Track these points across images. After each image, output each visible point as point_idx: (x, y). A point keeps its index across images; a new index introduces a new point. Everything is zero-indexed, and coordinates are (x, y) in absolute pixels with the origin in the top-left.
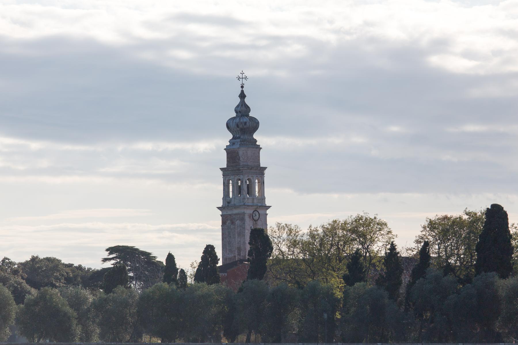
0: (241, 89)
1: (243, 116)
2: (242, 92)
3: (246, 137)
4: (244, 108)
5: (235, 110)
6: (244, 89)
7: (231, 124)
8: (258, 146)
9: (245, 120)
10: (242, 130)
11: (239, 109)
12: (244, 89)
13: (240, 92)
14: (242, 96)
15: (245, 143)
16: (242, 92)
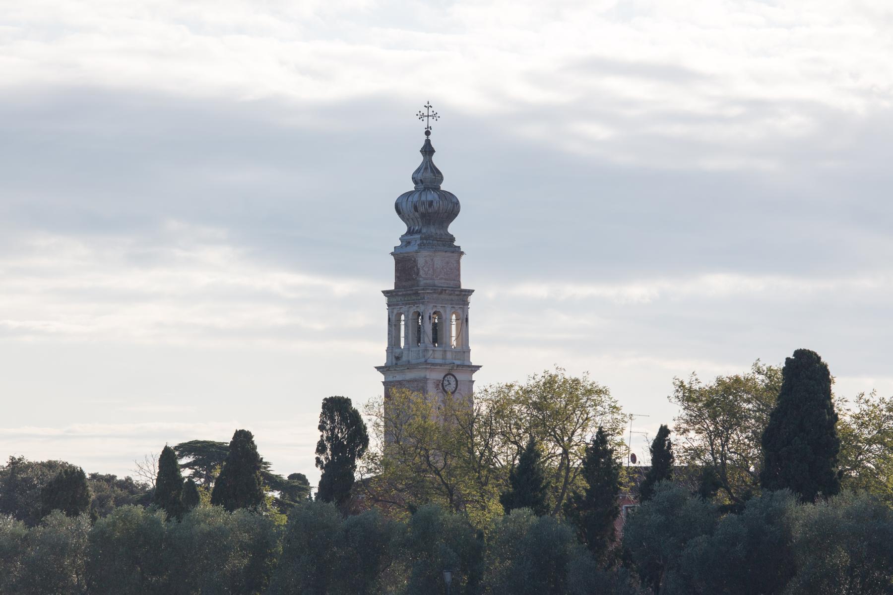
1: (427, 189)
4: (429, 175)
7: (404, 204)
11: (419, 176)
14: (428, 150)
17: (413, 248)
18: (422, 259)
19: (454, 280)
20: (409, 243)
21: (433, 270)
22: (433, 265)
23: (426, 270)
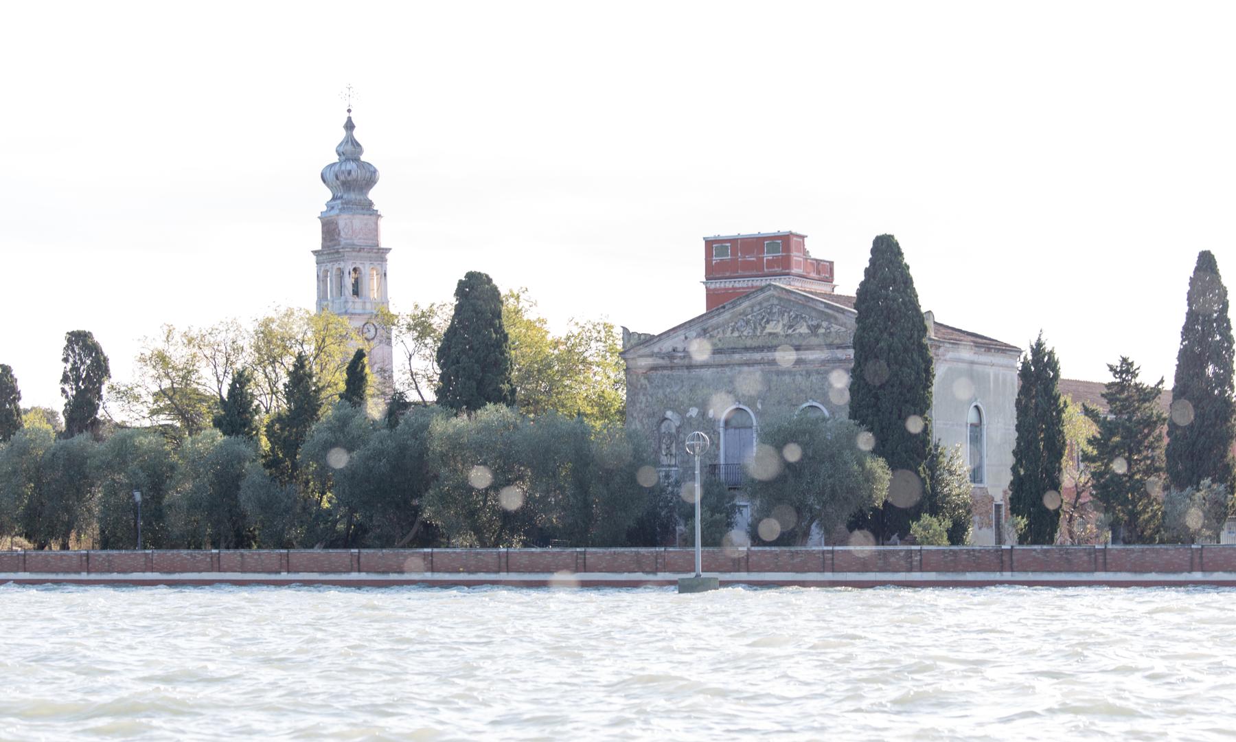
0: (347, 115)
1: (347, 160)
2: (349, 119)
3: (353, 196)
4: (349, 147)
9: (349, 167)
10: (344, 183)
11: (341, 149)
12: (352, 115)
13: (345, 120)
14: (350, 126)
16: (349, 119)
17: (336, 211)
18: (343, 221)
20: (333, 208)
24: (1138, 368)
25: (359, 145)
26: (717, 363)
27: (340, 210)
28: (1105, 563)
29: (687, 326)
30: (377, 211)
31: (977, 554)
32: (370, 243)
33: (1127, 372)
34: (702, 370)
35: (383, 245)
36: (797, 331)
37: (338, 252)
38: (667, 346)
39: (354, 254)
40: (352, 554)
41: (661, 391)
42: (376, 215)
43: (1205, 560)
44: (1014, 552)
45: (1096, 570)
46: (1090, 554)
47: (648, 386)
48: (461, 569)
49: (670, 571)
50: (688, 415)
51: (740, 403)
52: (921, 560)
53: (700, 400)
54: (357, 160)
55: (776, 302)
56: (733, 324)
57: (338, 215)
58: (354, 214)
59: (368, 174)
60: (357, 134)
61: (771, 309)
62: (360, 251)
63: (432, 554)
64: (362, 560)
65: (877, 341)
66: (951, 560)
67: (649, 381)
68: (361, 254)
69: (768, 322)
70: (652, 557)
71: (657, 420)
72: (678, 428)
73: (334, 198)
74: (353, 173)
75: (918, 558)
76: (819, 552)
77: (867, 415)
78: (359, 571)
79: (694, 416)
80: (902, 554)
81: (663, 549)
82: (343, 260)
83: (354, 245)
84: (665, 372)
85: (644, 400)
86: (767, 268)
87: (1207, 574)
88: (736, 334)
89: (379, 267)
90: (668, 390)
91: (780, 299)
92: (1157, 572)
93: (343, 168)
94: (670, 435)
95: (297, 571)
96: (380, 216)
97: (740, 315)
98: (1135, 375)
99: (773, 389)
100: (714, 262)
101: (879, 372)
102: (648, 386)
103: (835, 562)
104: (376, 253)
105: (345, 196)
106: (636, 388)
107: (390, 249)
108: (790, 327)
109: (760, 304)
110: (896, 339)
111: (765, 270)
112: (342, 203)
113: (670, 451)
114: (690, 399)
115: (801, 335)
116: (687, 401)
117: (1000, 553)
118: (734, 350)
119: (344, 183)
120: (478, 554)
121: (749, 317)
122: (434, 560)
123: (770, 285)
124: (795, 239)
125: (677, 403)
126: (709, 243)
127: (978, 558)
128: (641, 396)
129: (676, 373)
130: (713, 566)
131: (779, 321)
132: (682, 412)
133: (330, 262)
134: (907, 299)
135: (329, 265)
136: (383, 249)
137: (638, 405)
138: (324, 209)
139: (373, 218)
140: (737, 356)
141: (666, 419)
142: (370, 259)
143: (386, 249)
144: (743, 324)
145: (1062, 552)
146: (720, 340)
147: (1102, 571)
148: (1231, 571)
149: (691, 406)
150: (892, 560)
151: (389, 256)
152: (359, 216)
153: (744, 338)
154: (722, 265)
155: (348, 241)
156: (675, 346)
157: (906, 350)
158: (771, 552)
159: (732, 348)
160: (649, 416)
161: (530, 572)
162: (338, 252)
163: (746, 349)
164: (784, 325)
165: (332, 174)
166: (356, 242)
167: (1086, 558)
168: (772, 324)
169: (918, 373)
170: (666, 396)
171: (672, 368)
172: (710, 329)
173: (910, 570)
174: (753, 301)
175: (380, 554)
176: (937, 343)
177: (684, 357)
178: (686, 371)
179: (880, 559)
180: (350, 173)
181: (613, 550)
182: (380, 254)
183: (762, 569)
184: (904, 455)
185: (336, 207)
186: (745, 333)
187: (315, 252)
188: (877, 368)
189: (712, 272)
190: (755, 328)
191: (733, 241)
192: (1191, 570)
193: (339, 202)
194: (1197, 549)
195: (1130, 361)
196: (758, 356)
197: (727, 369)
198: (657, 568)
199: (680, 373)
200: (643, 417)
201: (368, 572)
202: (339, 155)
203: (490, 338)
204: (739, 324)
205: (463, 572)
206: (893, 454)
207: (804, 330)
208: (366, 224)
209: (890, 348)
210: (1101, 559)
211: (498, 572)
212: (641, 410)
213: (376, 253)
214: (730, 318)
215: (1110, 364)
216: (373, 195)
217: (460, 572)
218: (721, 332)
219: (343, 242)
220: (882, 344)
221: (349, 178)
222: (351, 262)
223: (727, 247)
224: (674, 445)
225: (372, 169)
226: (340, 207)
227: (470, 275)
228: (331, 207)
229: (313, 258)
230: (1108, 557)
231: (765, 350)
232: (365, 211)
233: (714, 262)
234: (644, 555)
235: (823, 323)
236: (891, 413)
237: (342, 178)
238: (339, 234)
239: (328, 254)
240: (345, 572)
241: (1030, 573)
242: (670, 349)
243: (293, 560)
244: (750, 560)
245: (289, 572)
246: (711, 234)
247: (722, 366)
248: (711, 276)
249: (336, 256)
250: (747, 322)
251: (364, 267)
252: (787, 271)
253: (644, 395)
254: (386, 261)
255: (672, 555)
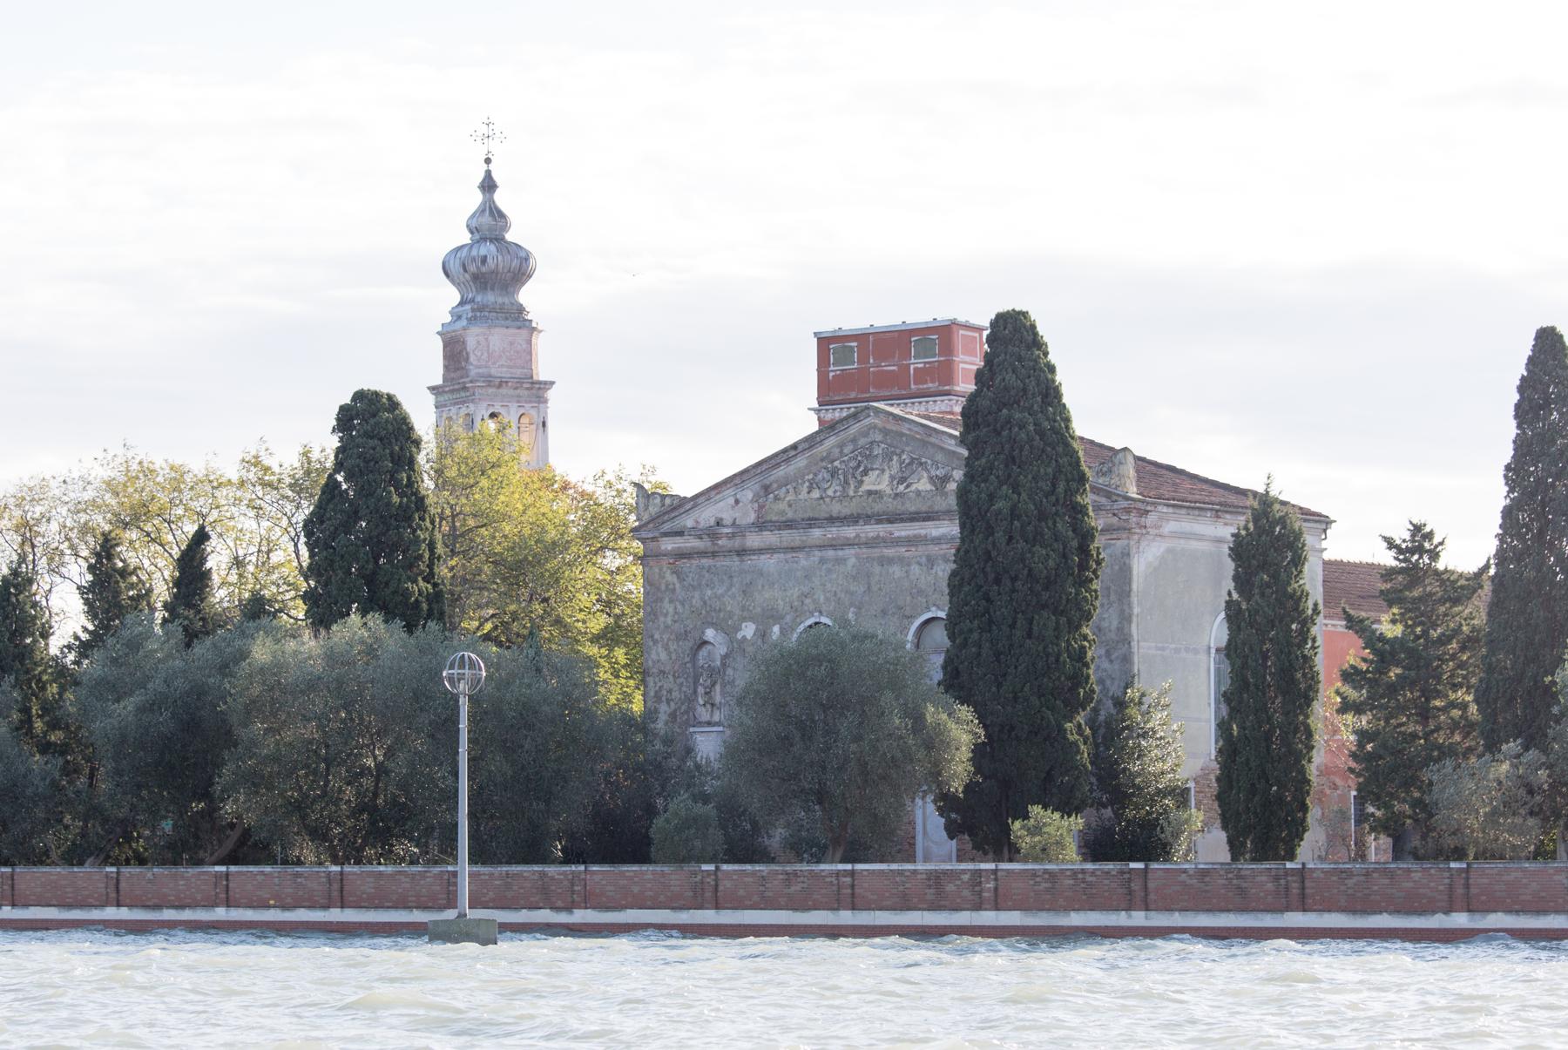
0: (485, 167)
1: (483, 239)
2: (488, 174)
3: (491, 298)
4: (486, 219)
5: (468, 226)
6: (491, 167)
7: (452, 262)
8: (527, 323)
9: (483, 251)
10: (476, 277)
11: (474, 224)
12: (491, 167)
13: (480, 176)
14: (488, 185)
15: (487, 314)
16: (488, 174)
17: (464, 322)
18: (473, 337)
19: (523, 368)
20: (459, 317)
21: (488, 353)
22: (488, 346)
23: (479, 354)
24: (1441, 543)
25: (502, 215)
26: (785, 544)
27: (469, 320)
28: (1303, 896)
29: (737, 481)
30: (531, 321)
31: (1089, 879)
32: (518, 372)
33: (1420, 550)
34: (762, 557)
35: (542, 374)
36: (913, 488)
37: (465, 389)
38: (706, 516)
39: (490, 390)
40: (107, 875)
41: (697, 594)
42: (530, 329)
43: (1474, 891)
44: (1150, 876)
45: (1288, 909)
46: (1277, 878)
47: (678, 586)
48: (272, 902)
49: (594, 908)
50: (739, 636)
51: (820, 612)
52: (996, 889)
53: (759, 610)
54: (498, 239)
55: (879, 437)
56: (811, 476)
57: (464, 329)
58: (489, 327)
59: (515, 263)
60: (500, 198)
61: (871, 449)
62: (500, 386)
63: (227, 874)
64: (123, 885)
65: (992, 497)
66: (1047, 890)
67: (678, 578)
68: (504, 391)
69: (865, 473)
70: (566, 883)
71: (691, 644)
72: (725, 657)
73: (462, 303)
74: (489, 260)
75: (991, 885)
76: (831, 873)
77: (971, 631)
78: (118, 905)
79: (749, 637)
80: (966, 877)
81: (582, 868)
82: (473, 401)
83: (490, 376)
84: (705, 562)
85: (671, 610)
86: (915, 384)
87: (1477, 916)
88: (816, 494)
89: (533, 412)
90: (709, 592)
91: (885, 432)
92: (1390, 913)
93: (474, 253)
94: (712, 672)
95: (26, 905)
96: (534, 329)
97: (822, 460)
98: (1434, 555)
99: (875, 588)
100: (831, 374)
101: (994, 554)
102: (678, 586)
103: (857, 891)
104: (527, 389)
105: (479, 299)
106: (658, 589)
107: (552, 383)
108: (902, 480)
109: (854, 440)
110: (1024, 496)
111: (913, 386)
112: (473, 310)
113: (711, 698)
114: (743, 608)
115: (918, 493)
116: (738, 612)
117: (1127, 876)
118: (812, 522)
119: (476, 277)
120: (298, 875)
121: (837, 463)
122: (231, 885)
123: (867, 408)
124: (961, 332)
125: (722, 615)
126: (826, 343)
127: (1090, 885)
128: (666, 604)
129: (722, 562)
130: (662, 898)
131: (883, 471)
132: (729, 631)
133: (455, 404)
134: (1047, 425)
135: (454, 409)
136: (540, 383)
137: (662, 619)
138: (448, 319)
139: (524, 332)
140: (817, 533)
141: (706, 643)
142: (518, 399)
143: (545, 383)
144: (827, 476)
145: (1230, 876)
146: (790, 506)
147: (1296, 910)
148: (1517, 912)
149: (744, 619)
150: (950, 888)
151: (551, 394)
152: (497, 330)
153: (827, 500)
154: (844, 378)
155: (481, 371)
156: (719, 516)
157: (1042, 516)
158: (754, 873)
159: (810, 519)
160: (678, 639)
161: (377, 907)
162: (465, 389)
163: (832, 520)
164: (892, 478)
165: (458, 261)
166: (493, 371)
167: (1270, 886)
168: (873, 475)
169: (1064, 556)
170: (705, 603)
171: (714, 554)
172: (775, 486)
173: (978, 907)
174: (843, 435)
175: (149, 875)
176: (1140, 505)
177: (734, 535)
178: (736, 559)
179: (930, 887)
180: (484, 260)
181: (505, 868)
182: (536, 391)
183: (739, 905)
184: (1035, 701)
185: (465, 316)
186: (830, 492)
187: (433, 389)
188: (990, 547)
189: (829, 391)
190: (846, 482)
191: (861, 337)
192: (1448, 911)
193: (468, 307)
194: (1460, 870)
195: (1427, 529)
196: (850, 532)
197: (801, 555)
198: (573, 902)
199: (727, 562)
200: (669, 639)
201: (131, 906)
202: (472, 233)
203: (389, 504)
204: (820, 476)
205: (274, 906)
206: (1016, 698)
207: (924, 485)
208: (511, 344)
209: (1014, 514)
210: (1295, 888)
211: (326, 907)
212: (667, 627)
213: (527, 389)
214: (807, 467)
215: (1388, 535)
216: (527, 296)
217: (269, 907)
218: (791, 490)
219: (473, 372)
220: (1000, 504)
221: (484, 269)
222: (485, 404)
223: (852, 348)
224: (718, 687)
225: (523, 254)
226: (470, 315)
227: (360, 396)
228: (457, 317)
229: (431, 399)
230: (1308, 884)
231: (861, 522)
232: (509, 323)
233: (831, 374)
234: (552, 878)
235: (955, 472)
236: (1013, 626)
237: (472, 268)
238: (467, 359)
239: (452, 391)
240: (96, 907)
241: (1177, 914)
242: (712, 522)
243: (21, 886)
244: (721, 888)
245: (13, 905)
246: (828, 326)
247: (793, 549)
248: (828, 398)
249: (463, 394)
250: (834, 473)
251: (509, 413)
252: (947, 388)
253: (671, 601)
254: (546, 401)
255: (597, 878)
